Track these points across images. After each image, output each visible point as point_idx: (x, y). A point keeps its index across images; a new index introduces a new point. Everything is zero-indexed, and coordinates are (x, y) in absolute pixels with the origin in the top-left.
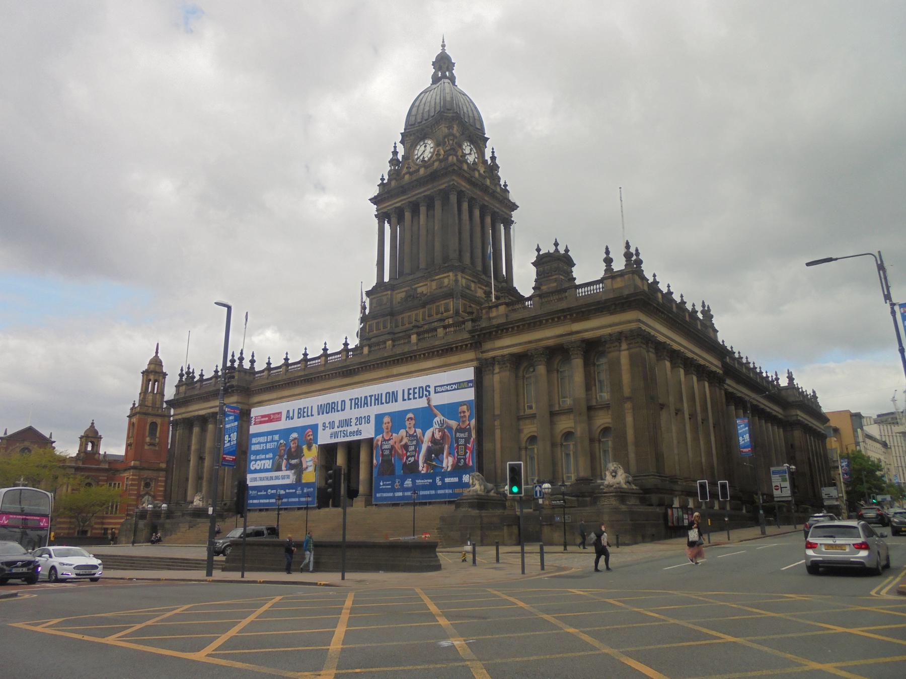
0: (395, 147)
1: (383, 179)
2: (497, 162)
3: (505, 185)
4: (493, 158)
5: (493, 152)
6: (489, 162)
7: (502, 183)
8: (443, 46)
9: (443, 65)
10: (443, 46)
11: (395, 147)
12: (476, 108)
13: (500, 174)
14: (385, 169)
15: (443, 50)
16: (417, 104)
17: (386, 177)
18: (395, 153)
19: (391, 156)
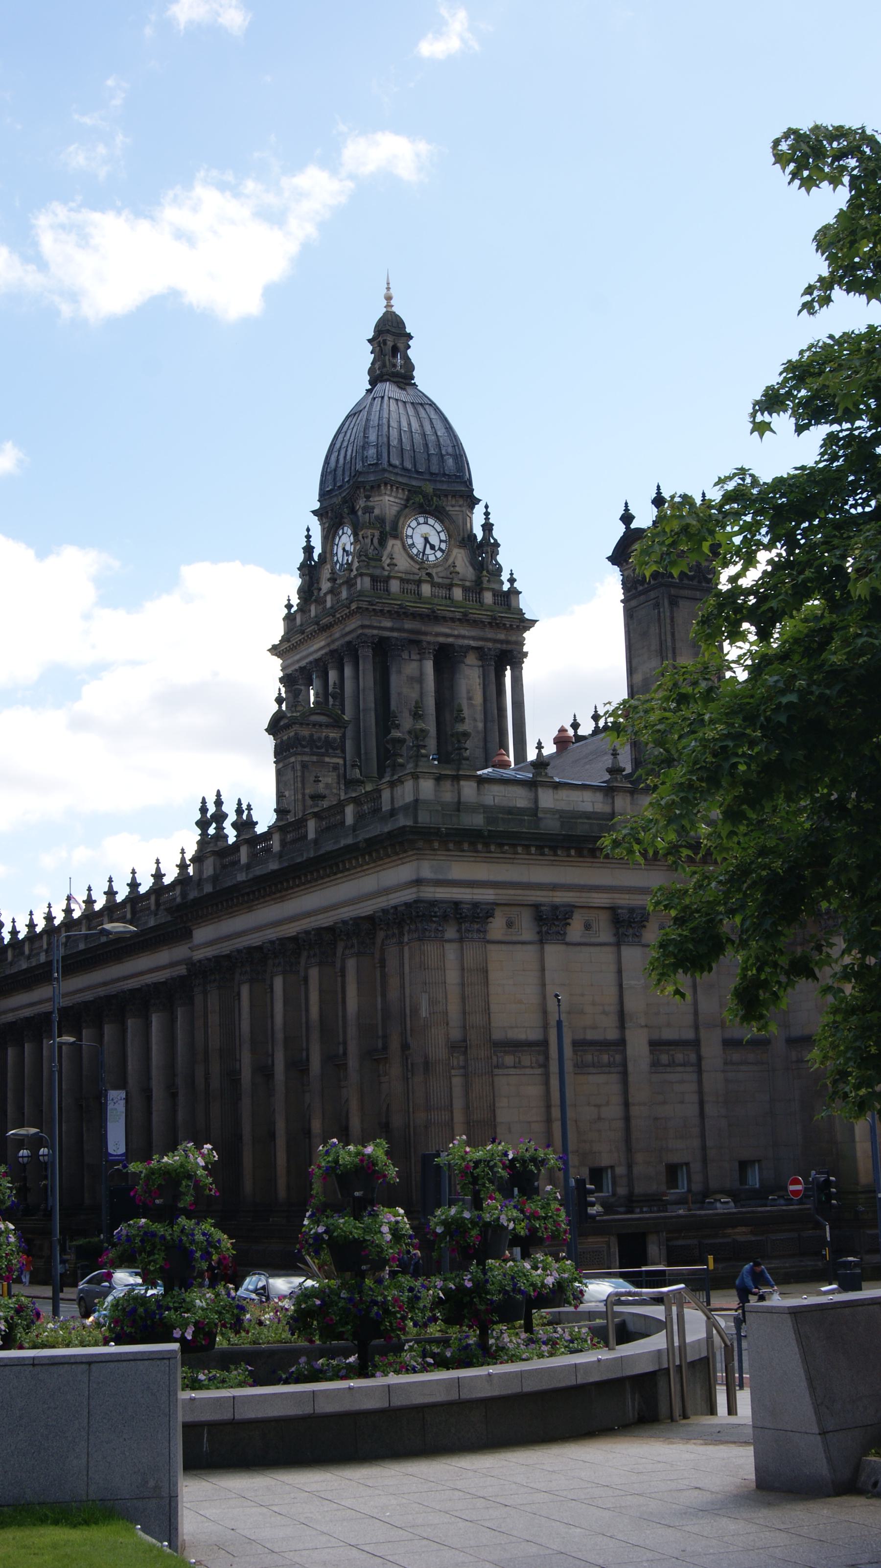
0: (308, 537)
1: (289, 606)
2: (495, 533)
3: (512, 580)
4: (488, 527)
5: (487, 514)
6: (480, 536)
7: (505, 576)
8: (389, 298)
9: (390, 340)
10: (389, 298)
11: (308, 537)
12: (449, 428)
13: (501, 558)
14: (289, 586)
15: (389, 306)
16: (338, 445)
17: (295, 601)
18: (308, 550)
19: (300, 557)
